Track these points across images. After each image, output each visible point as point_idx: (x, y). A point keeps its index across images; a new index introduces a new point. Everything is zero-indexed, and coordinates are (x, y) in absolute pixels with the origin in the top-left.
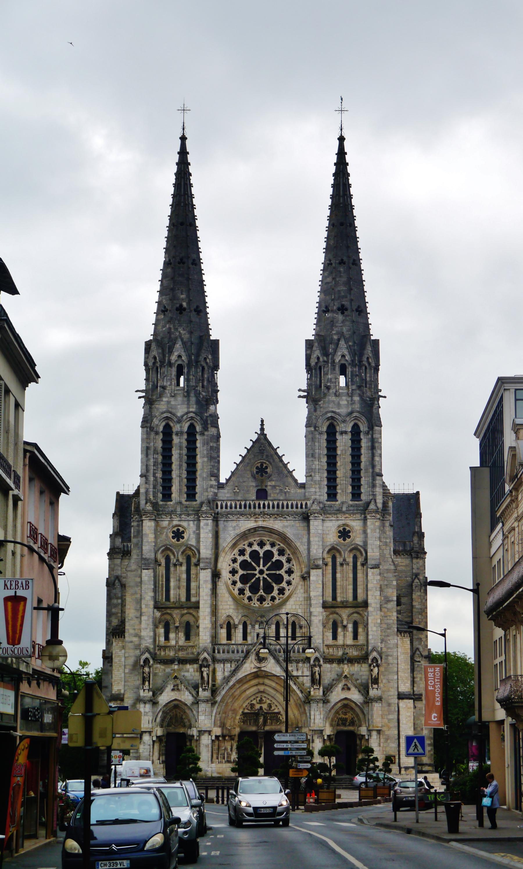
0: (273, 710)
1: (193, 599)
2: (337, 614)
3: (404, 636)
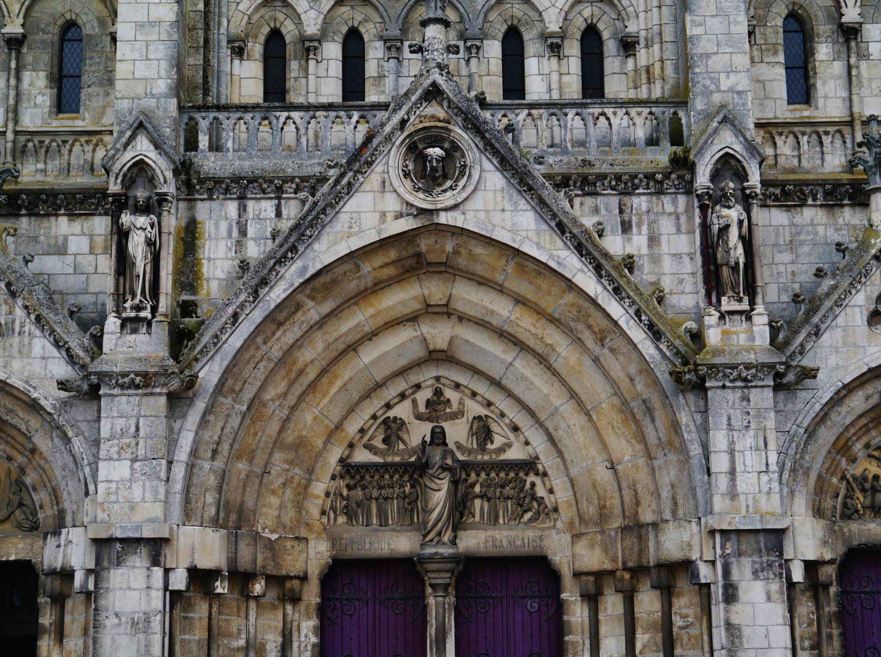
0: (502, 450)
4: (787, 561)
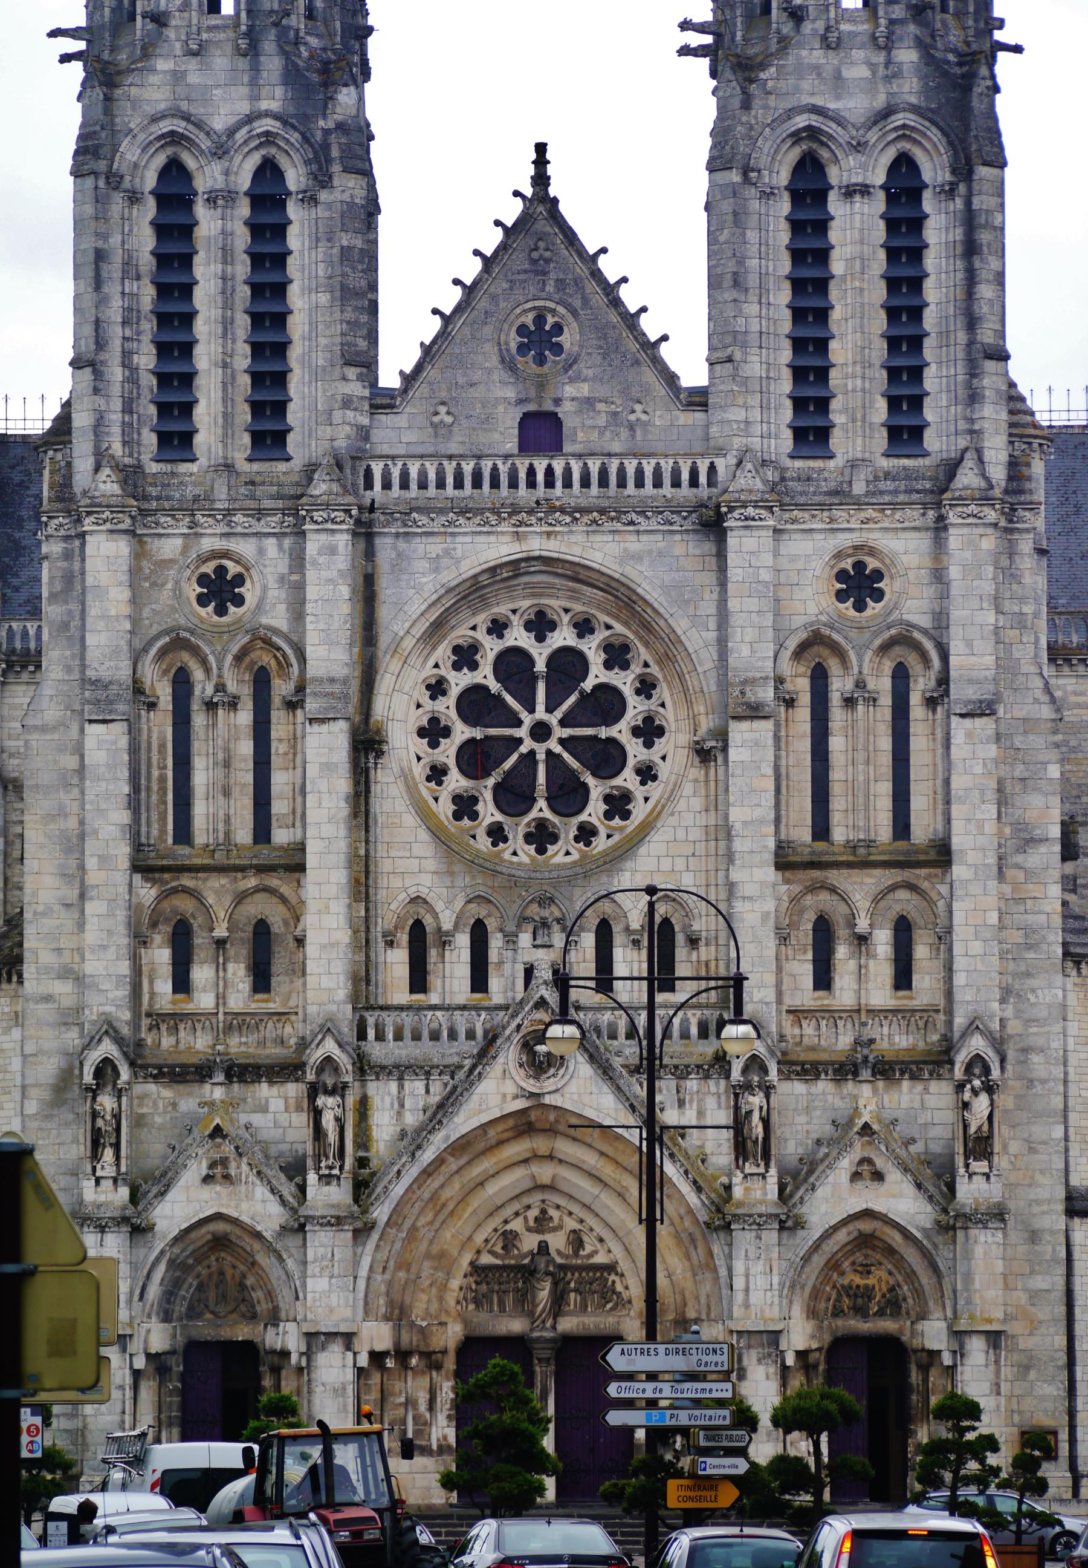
0: (591, 1255)
1: (281, 836)
2: (833, 890)
4: (782, 1352)
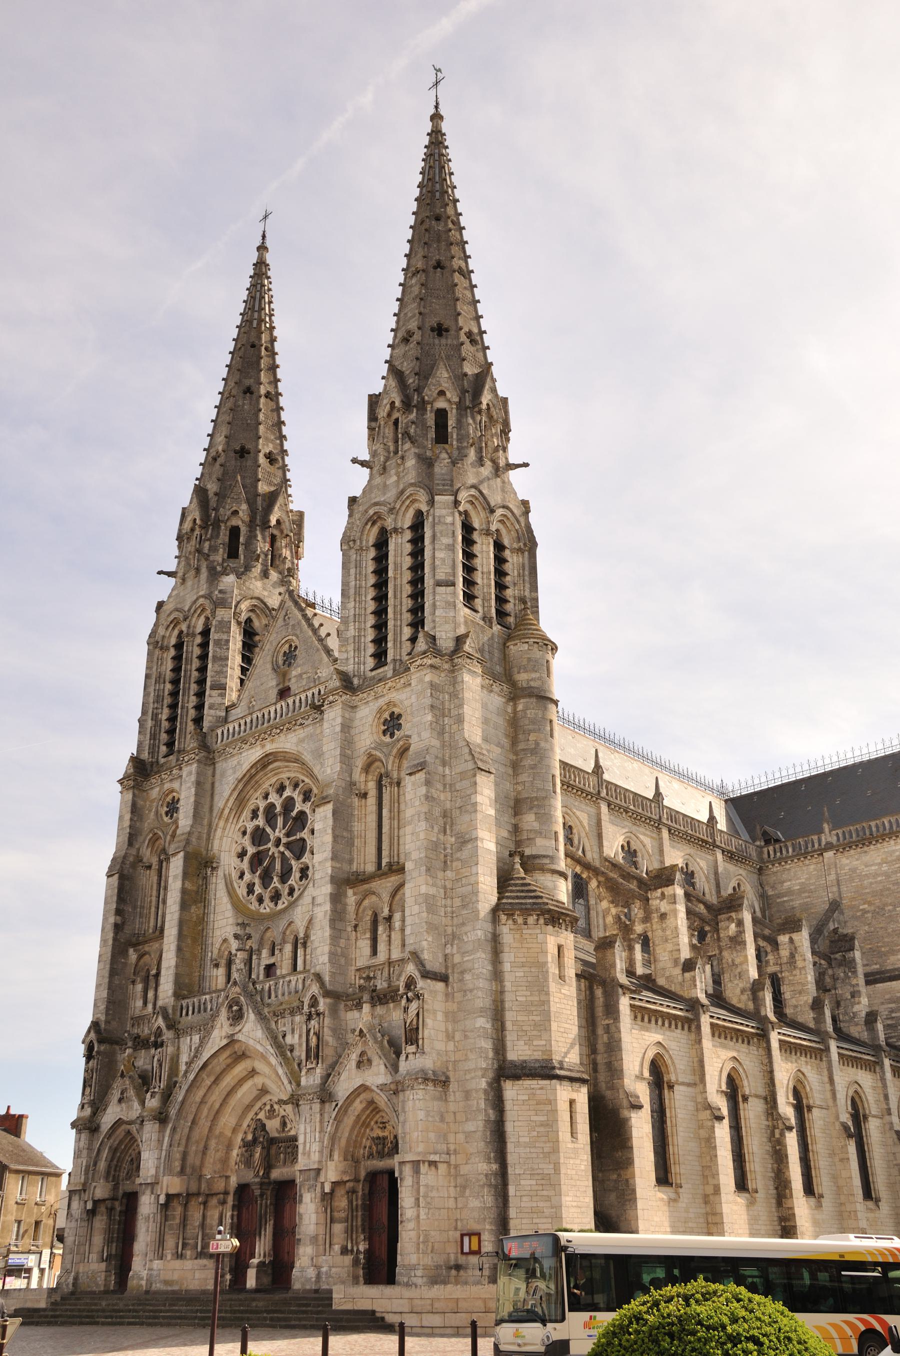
0: (289, 1131)
3: (525, 923)
